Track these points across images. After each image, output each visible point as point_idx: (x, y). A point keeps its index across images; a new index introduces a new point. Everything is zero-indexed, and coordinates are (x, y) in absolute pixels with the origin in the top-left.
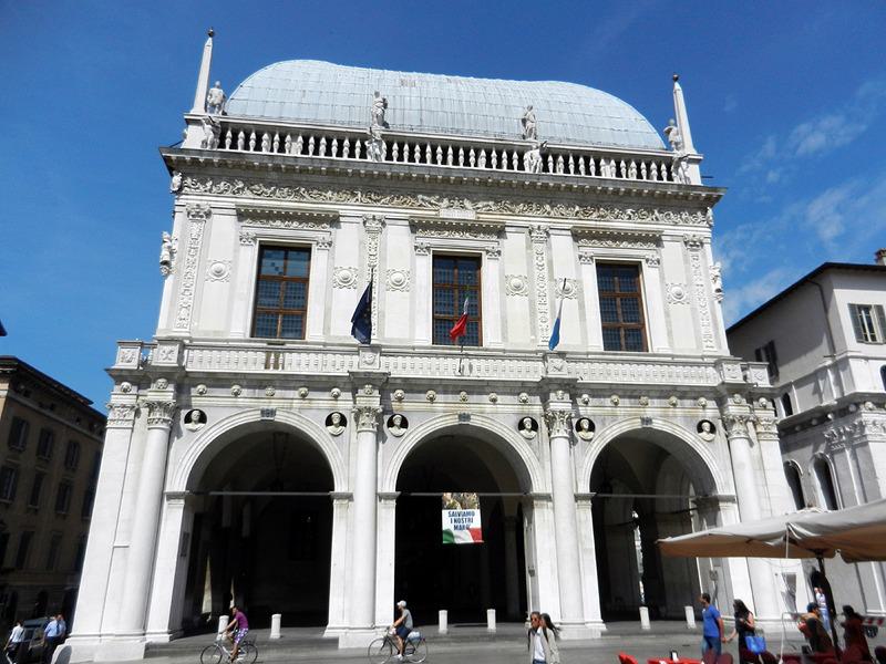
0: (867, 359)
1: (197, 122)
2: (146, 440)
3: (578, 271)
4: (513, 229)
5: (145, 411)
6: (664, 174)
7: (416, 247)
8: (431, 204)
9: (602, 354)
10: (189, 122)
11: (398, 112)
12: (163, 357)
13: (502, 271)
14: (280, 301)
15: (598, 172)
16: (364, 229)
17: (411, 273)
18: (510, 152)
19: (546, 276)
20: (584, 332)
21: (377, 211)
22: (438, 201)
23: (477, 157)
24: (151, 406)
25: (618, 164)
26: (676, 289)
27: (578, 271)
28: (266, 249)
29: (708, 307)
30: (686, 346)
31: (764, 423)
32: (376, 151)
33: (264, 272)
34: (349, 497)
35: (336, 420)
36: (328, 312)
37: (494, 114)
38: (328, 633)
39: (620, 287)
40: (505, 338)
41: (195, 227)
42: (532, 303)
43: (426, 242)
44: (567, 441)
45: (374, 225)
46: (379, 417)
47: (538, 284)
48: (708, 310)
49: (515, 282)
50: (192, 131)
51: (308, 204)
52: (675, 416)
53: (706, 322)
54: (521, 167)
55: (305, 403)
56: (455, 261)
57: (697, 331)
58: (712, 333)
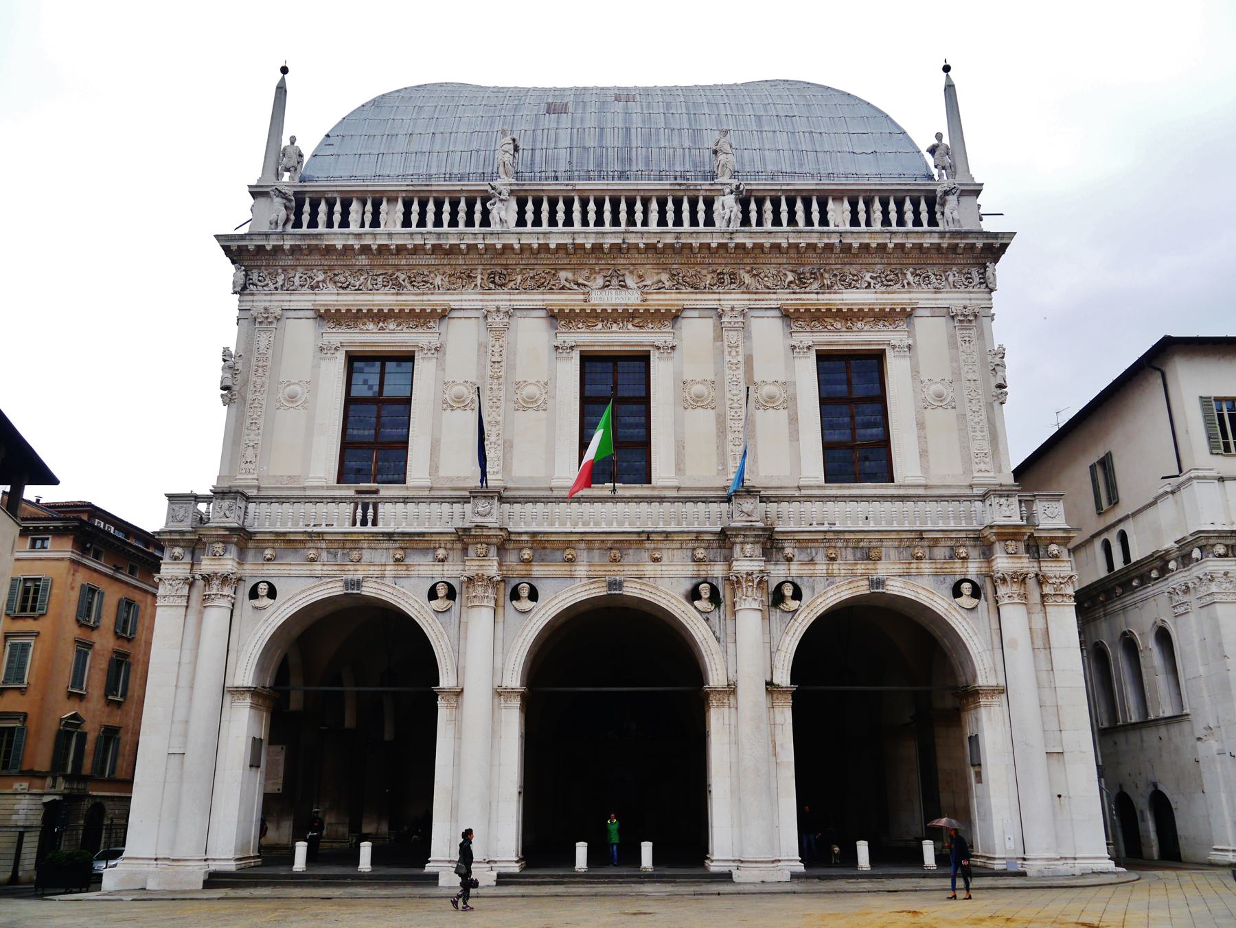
0: (1222, 479)
2: (201, 619)
4: (696, 314)
5: (201, 583)
6: (924, 217)
7: (557, 348)
8: (578, 284)
9: (819, 487)
11: (538, 152)
15: (824, 221)
16: (483, 327)
18: (691, 203)
20: (797, 458)
21: (502, 299)
22: (588, 279)
23: (646, 213)
24: (207, 579)
26: (935, 388)
28: (354, 360)
29: (983, 412)
30: (948, 470)
31: (1054, 580)
33: (354, 394)
35: (442, 591)
36: (437, 447)
37: (676, 143)
38: (429, 868)
40: (679, 469)
41: (264, 339)
44: (759, 614)
45: (497, 320)
49: (697, 389)
51: (411, 299)
52: (920, 575)
53: (978, 434)
54: (709, 222)
55: (401, 571)
56: (615, 365)
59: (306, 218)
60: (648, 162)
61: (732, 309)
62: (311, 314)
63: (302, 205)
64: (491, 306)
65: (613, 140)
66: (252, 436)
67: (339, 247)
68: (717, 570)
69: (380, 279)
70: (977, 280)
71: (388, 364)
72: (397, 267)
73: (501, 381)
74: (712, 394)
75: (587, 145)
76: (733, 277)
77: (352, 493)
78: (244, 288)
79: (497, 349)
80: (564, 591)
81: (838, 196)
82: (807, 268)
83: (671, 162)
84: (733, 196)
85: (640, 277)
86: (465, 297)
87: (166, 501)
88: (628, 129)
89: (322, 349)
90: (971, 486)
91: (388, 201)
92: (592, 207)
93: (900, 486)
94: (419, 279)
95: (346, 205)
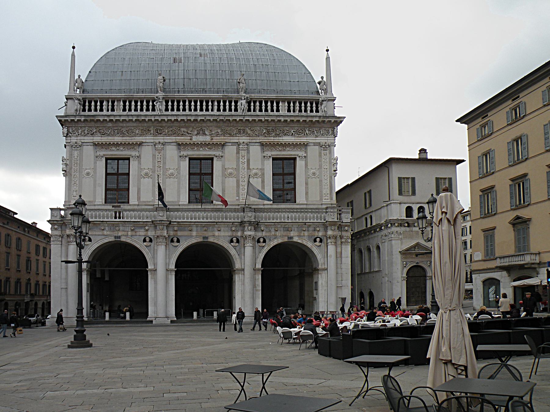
3: (263, 164)
4: (230, 144)
8: (188, 133)
13: (223, 166)
15: (278, 110)
19: (246, 168)
21: (160, 139)
22: (191, 131)
25: (289, 104)
27: (263, 164)
29: (328, 179)
30: (314, 199)
32: (160, 106)
33: (108, 172)
36: (141, 192)
37: (224, 77)
41: (76, 153)
42: (238, 182)
43: (185, 153)
45: (159, 146)
48: (328, 181)
49: (229, 171)
51: (127, 139)
54: (236, 110)
57: (321, 192)
58: (329, 192)
59: (87, 108)
61: (243, 143)
62: (92, 144)
63: (85, 103)
64: (157, 141)
66: (75, 188)
67: (102, 120)
69: (116, 131)
70: (331, 133)
71: (120, 161)
72: (122, 127)
73: (161, 168)
74: (235, 173)
75: (190, 77)
76: (244, 130)
78: (67, 134)
79: (159, 157)
81: (283, 101)
82: (271, 128)
84: (245, 101)
85: (210, 130)
86: (147, 138)
87: (50, 210)
89: (97, 157)
90: (322, 204)
91: (117, 101)
92: (193, 103)
93: (298, 204)
94: (130, 131)
95: (102, 103)
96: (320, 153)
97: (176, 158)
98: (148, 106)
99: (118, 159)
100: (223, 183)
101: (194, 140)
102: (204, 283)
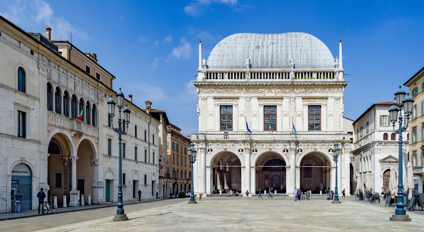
1: (200, 72)
3: (303, 109)
5: (199, 149)
10: (198, 72)
12: (201, 137)
14: (226, 122)
17: (258, 112)
18: (285, 74)
21: (248, 95)
24: (201, 149)
25: (318, 74)
26: (330, 113)
27: (303, 109)
32: (248, 76)
34: (245, 167)
39: (315, 111)
40: (282, 128)
41: (204, 102)
43: (262, 103)
45: (248, 99)
46: (250, 150)
47: (292, 112)
49: (285, 113)
50: (199, 74)
54: (289, 78)
55: (234, 147)
58: (339, 124)
59: (209, 77)
60: (277, 63)
63: (208, 75)
64: (247, 96)
65: (270, 57)
68: (288, 147)
77: (223, 133)
80: (262, 150)
81: (315, 72)
83: (282, 63)
88: (273, 54)
96: (334, 102)
97: (257, 105)
98: (241, 76)
99: (227, 106)
100: (282, 119)
101: (266, 95)
102: (271, 173)
